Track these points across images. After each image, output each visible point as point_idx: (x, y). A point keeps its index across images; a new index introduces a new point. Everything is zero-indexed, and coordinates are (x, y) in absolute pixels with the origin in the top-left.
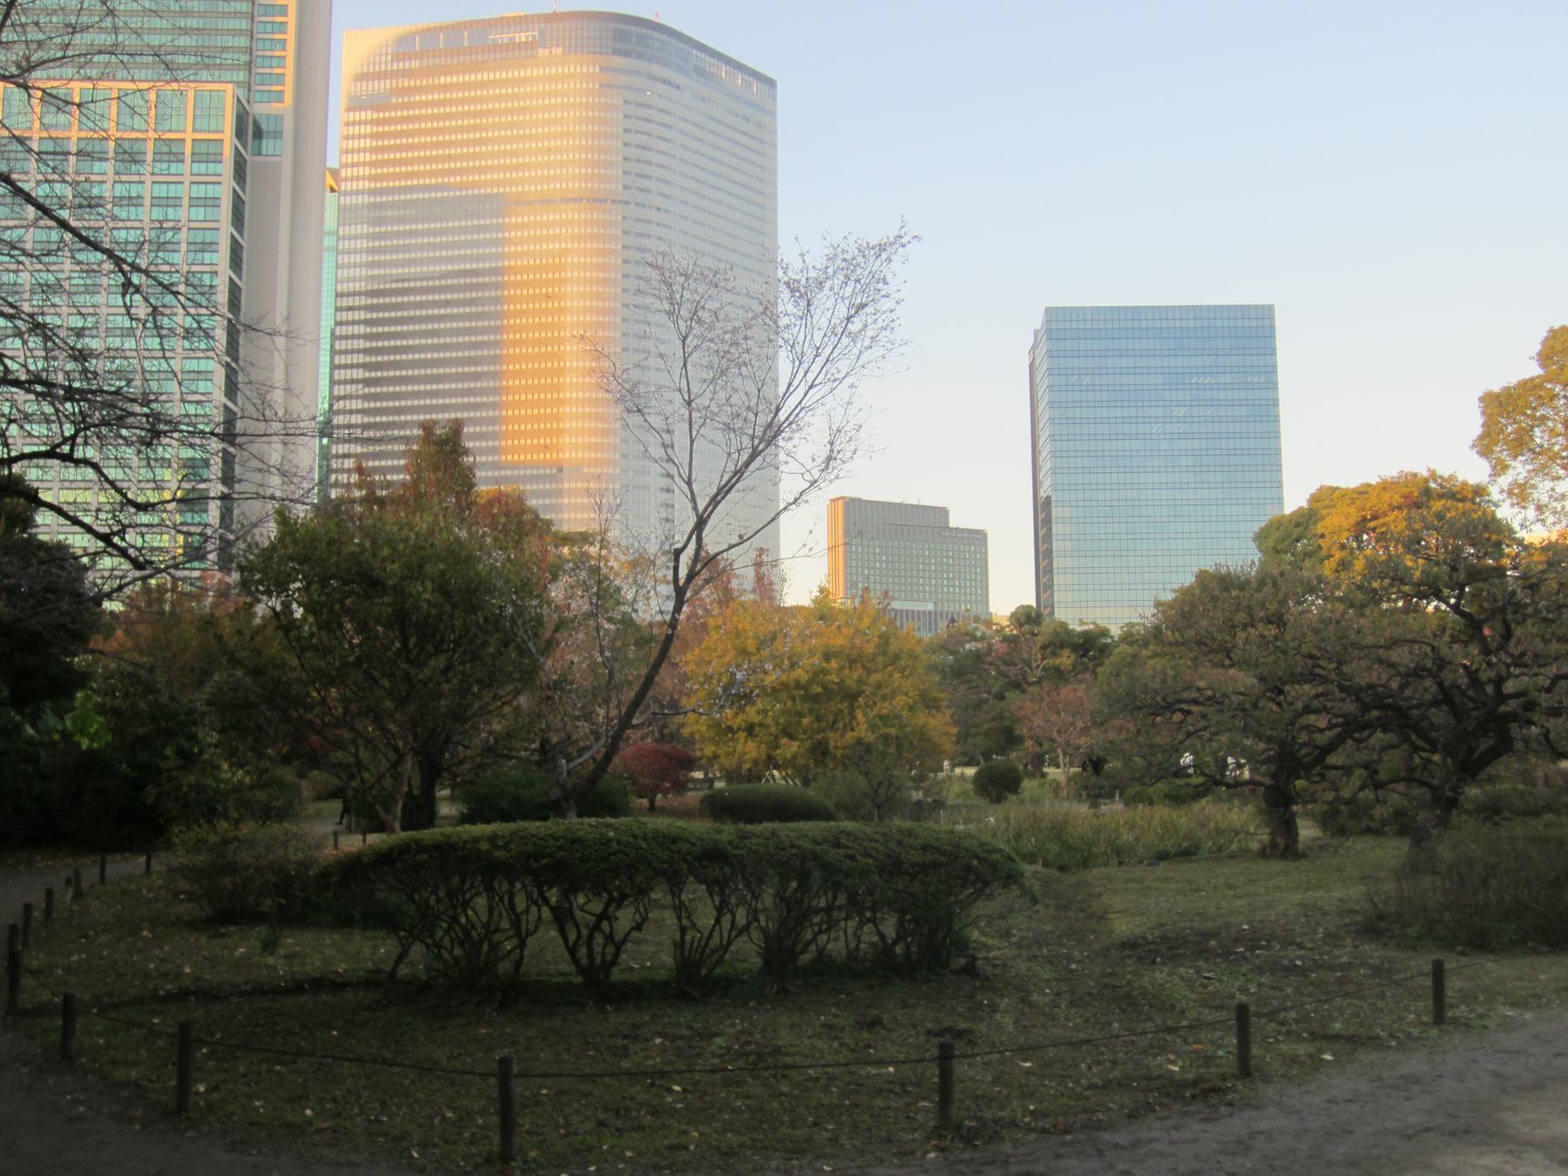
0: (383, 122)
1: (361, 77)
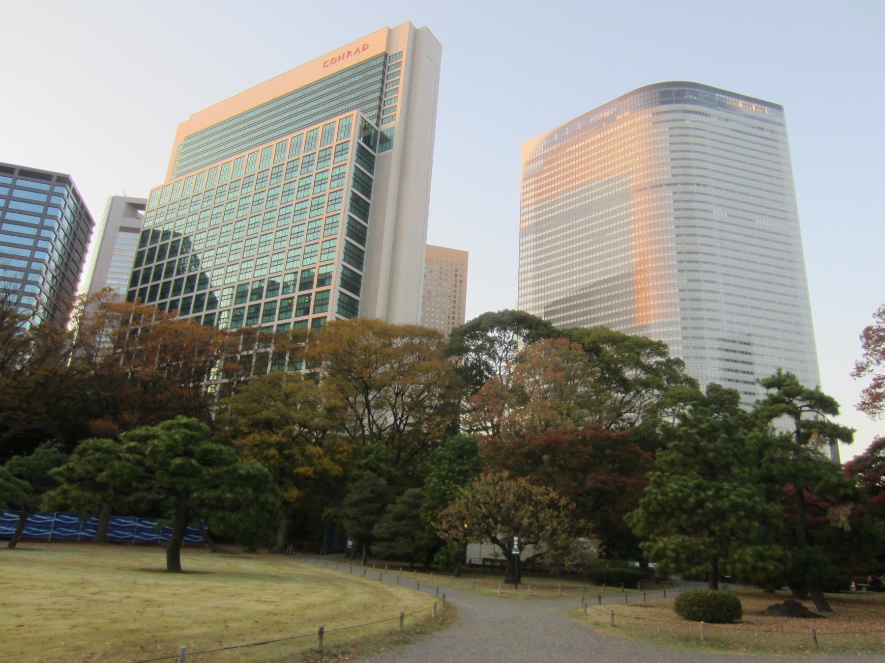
1: (529, 163)
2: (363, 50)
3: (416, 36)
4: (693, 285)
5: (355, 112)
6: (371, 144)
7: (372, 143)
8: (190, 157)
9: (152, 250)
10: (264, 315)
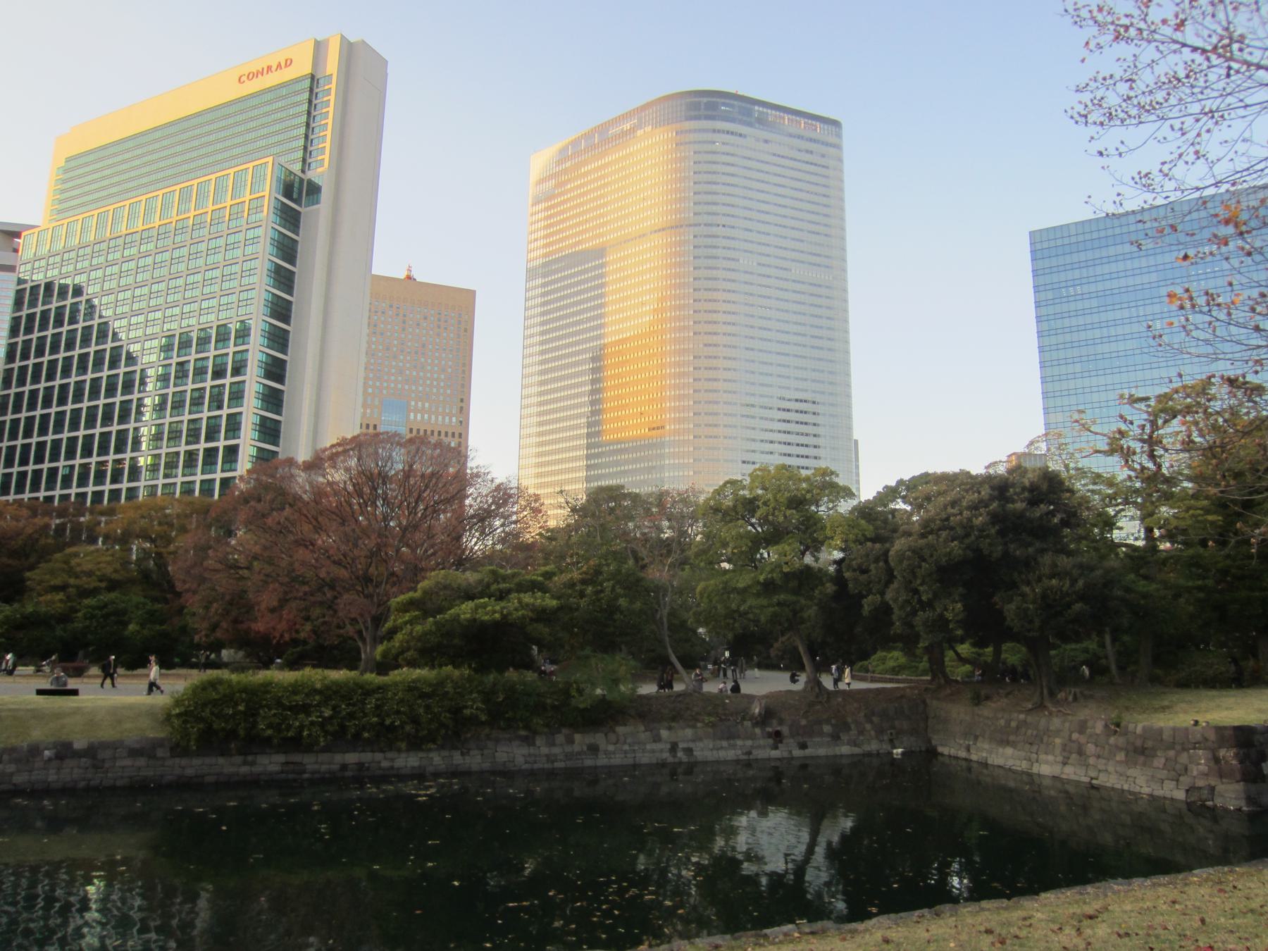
0: (553, 207)
1: (542, 181)
2: (286, 66)
3: (350, 51)
4: (711, 351)
5: (270, 159)
6: (295, 196)
7: (296, 194)
8: (73, 188)
9: (31, 318)
10: (172, 408)
